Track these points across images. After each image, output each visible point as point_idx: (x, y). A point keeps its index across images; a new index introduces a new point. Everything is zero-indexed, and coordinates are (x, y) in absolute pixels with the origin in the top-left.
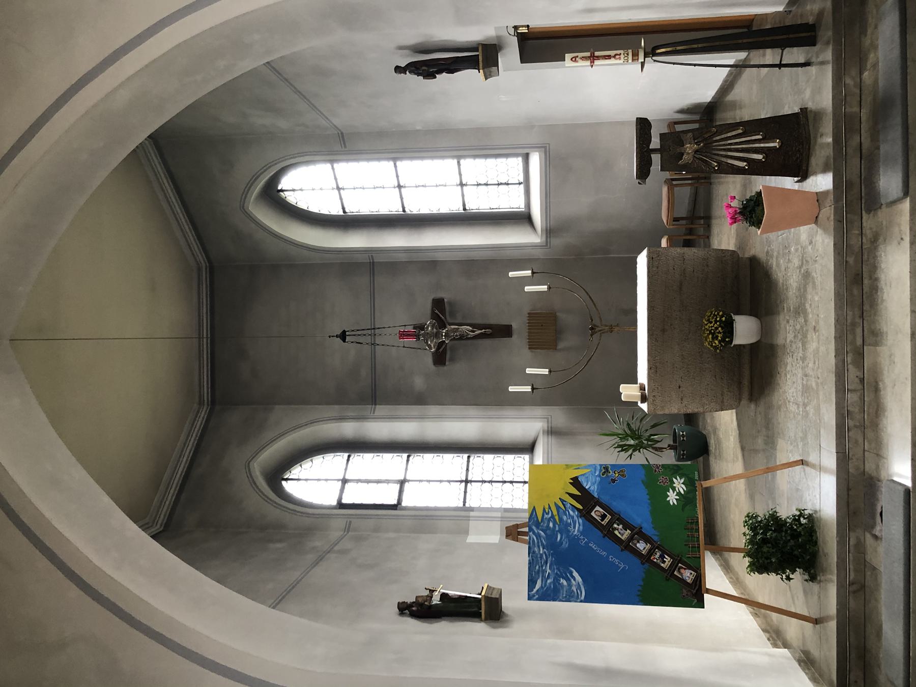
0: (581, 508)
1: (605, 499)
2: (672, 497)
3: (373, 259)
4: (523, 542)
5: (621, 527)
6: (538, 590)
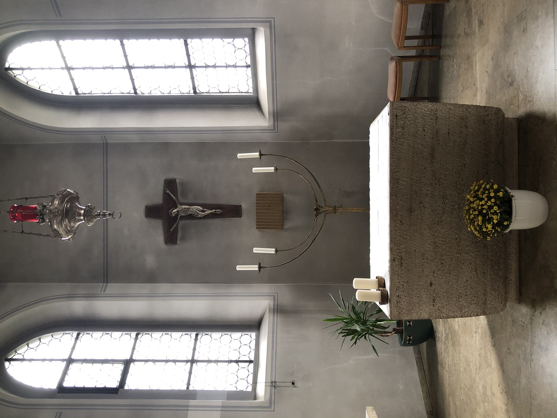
3: (106, 140)
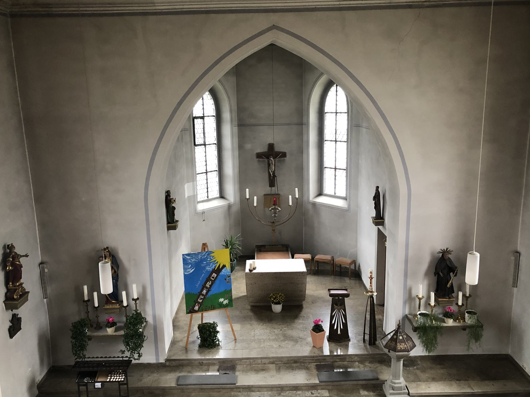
0: (216, 269)
1: (219, 277)
2: (221, 300)
3: (304, 125)
4: (202, 250)
5: (210, 284)
6: (186, 257)
